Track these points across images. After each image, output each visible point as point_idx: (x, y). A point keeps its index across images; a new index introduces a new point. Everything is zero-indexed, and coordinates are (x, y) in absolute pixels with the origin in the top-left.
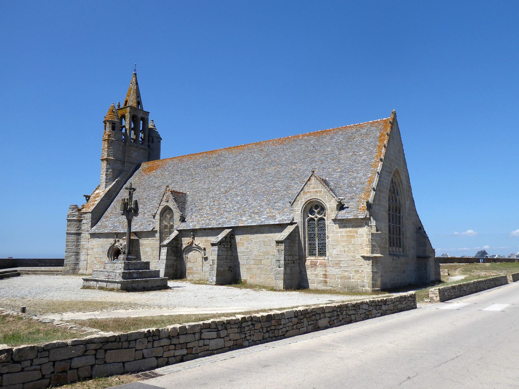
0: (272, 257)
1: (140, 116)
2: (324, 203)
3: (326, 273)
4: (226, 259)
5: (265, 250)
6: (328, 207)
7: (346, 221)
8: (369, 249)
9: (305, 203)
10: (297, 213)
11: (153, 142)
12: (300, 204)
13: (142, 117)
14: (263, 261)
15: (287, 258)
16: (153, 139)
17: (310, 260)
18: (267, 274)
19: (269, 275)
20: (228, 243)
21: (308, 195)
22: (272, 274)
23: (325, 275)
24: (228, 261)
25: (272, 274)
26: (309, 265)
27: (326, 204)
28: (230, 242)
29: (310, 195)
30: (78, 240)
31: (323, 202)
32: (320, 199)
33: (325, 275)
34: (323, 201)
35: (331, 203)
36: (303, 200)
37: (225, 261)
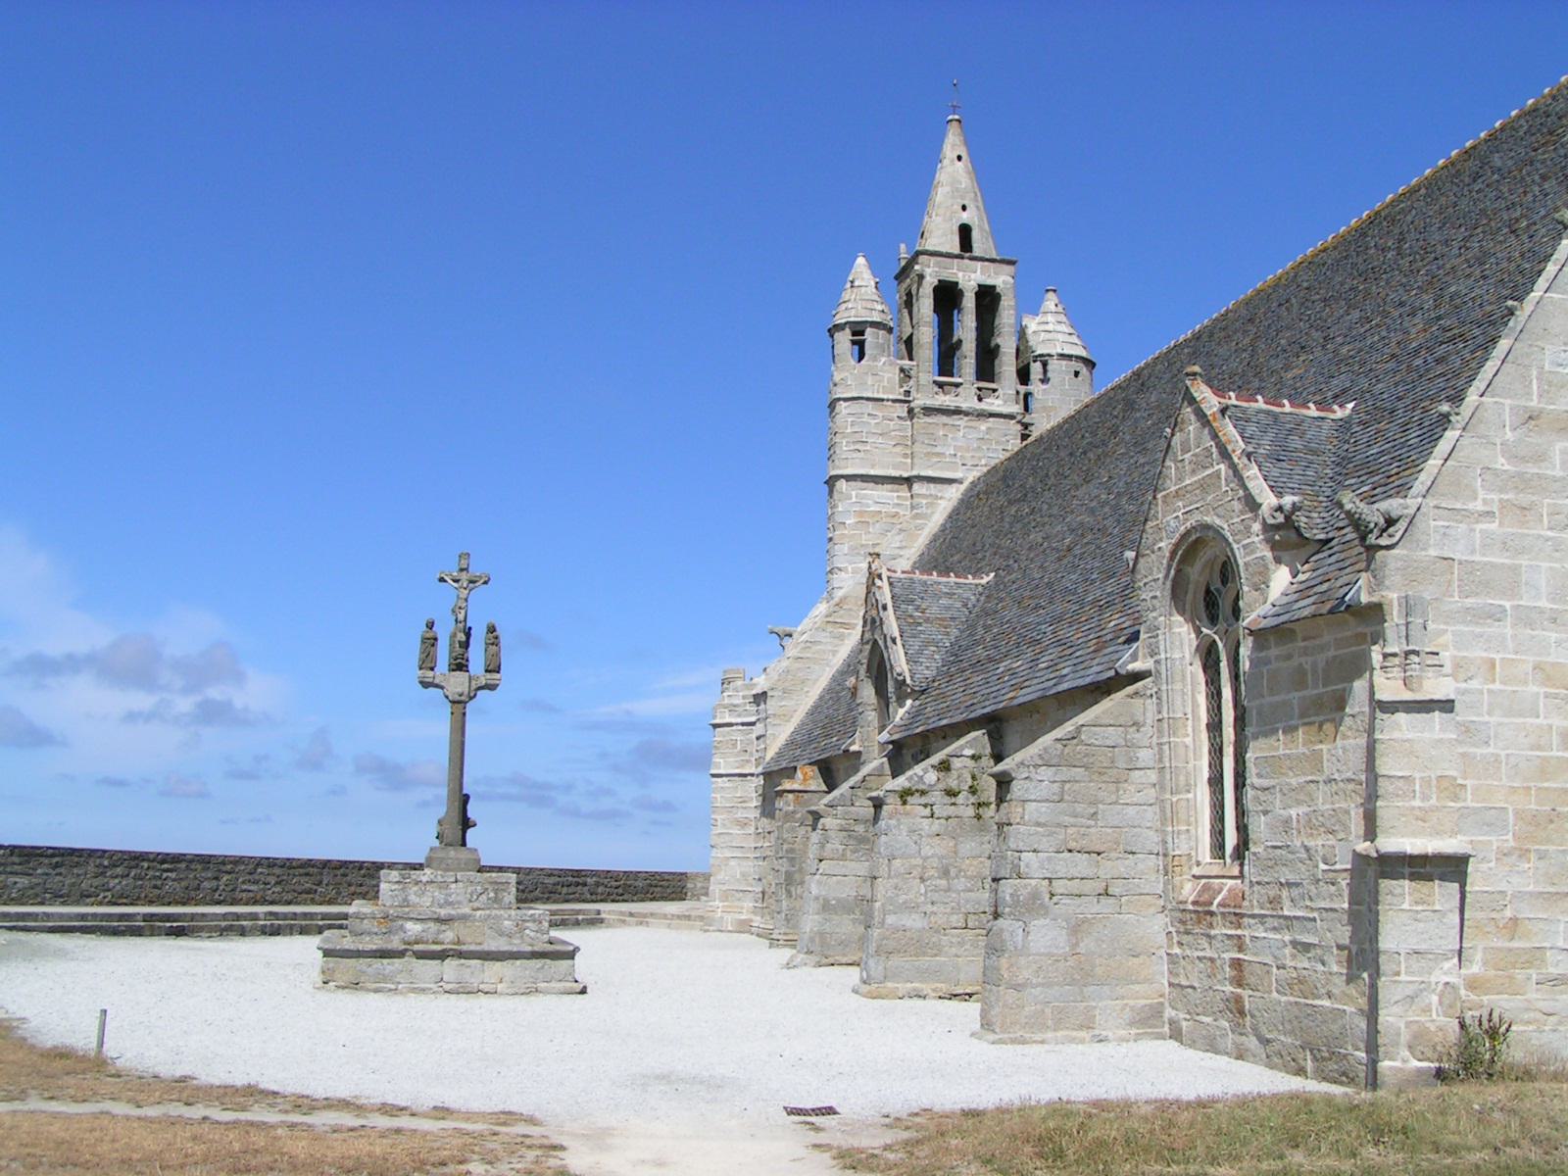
1: (972, 283)
3: (1241, 956)
4: (945, 873)
7: (1304, 640)
9: (1172, 559)
11: (1045, 380)
13: (979, 286)
15: (1035, 865)
16: (1045, 365)
17: (1203, 881)
20: (960, 799)
23: (1237, 964)
24: (961, 884)
26: (1191, 907)
27: (1235, 546)
28: (973, 790)
29: (1184, 507)
30: (744, 802)
32: (1218, 521)
33: (1237, 964)
37: (943, 883)
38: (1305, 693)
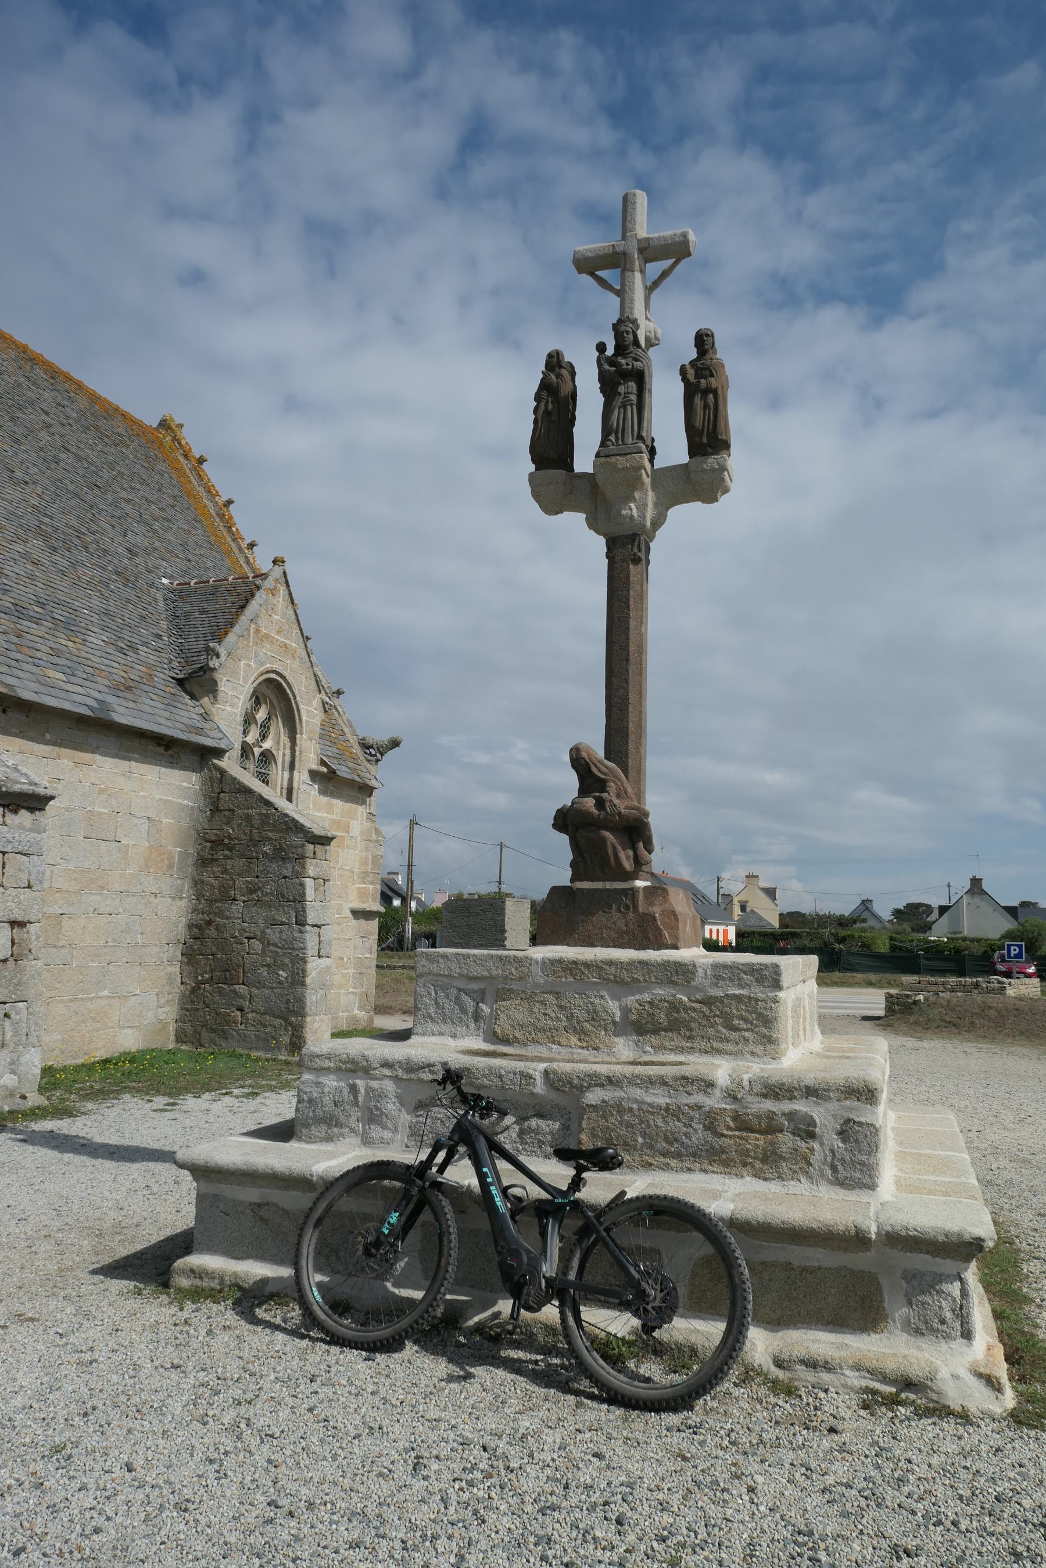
0: (117, 902)
2: (296, 703)
5: (87, 865)
6: (304, 718)
8: (371, 887)
10: (228, 708)
12: (244, 678)
14: (66, 923)
18: (82, 999)
19: (91, 999)
21: (266, 650)
22: (106, 993)
25: (106, 993)
27: (301, 706)
31: (295, 698)
34: (296, 691)
35: (312, 709)
36: (252, 664)
38: (331, 816)
